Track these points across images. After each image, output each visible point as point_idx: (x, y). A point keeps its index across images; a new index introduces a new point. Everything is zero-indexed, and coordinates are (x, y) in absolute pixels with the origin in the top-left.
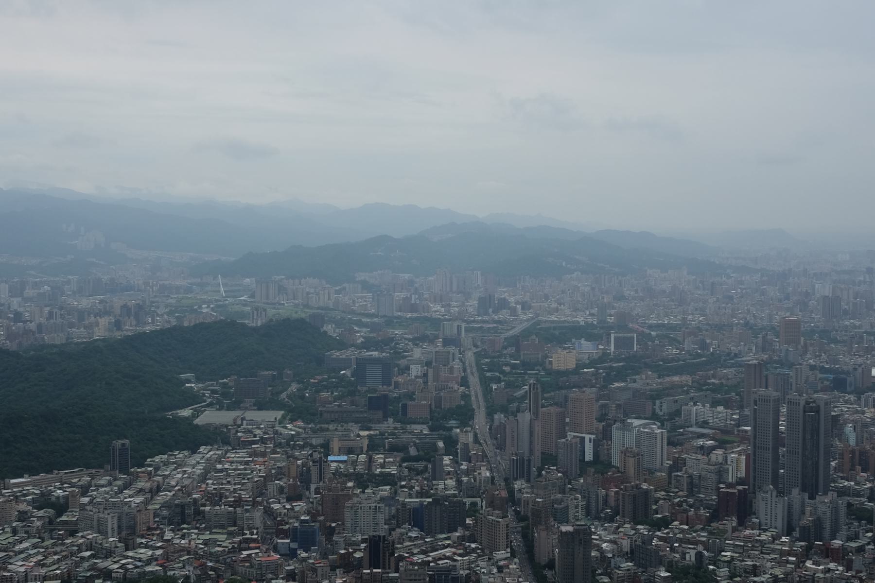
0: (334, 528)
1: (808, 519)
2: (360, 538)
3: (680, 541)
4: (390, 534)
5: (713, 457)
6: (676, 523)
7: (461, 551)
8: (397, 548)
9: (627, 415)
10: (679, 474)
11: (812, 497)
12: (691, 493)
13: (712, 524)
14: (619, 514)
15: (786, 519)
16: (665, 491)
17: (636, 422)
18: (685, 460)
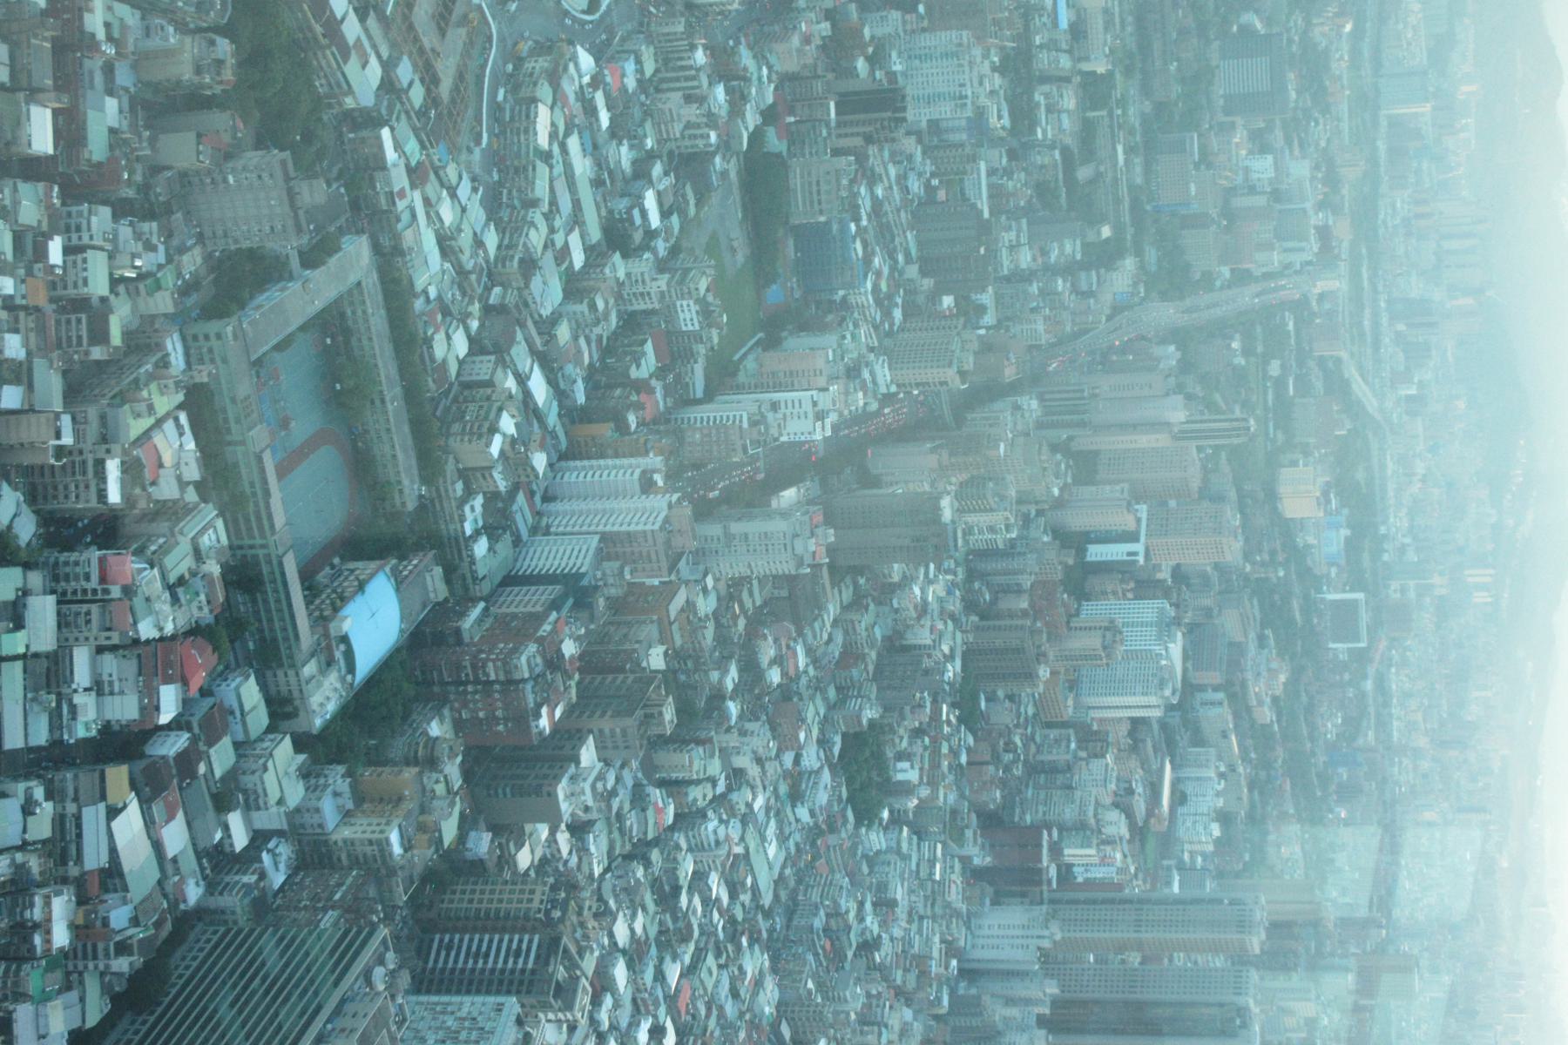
0: (915, 10)
1: (999, 1013)
2: (897, 68)
3: (935, 751)
4: (908, 133)
5: (1114, 815)
6: (971, 740)
7: (884, 286)
8: (881, 150)
9: (1192, 630)
10: (1073, 745)
11: (1042, 1021)
12: (1033, 769)
13: (974, 817)
14: (982, 618)
15: (989, 966)
16: (1035, 715)
17: (1176, 649)
18: (1103, 756)
